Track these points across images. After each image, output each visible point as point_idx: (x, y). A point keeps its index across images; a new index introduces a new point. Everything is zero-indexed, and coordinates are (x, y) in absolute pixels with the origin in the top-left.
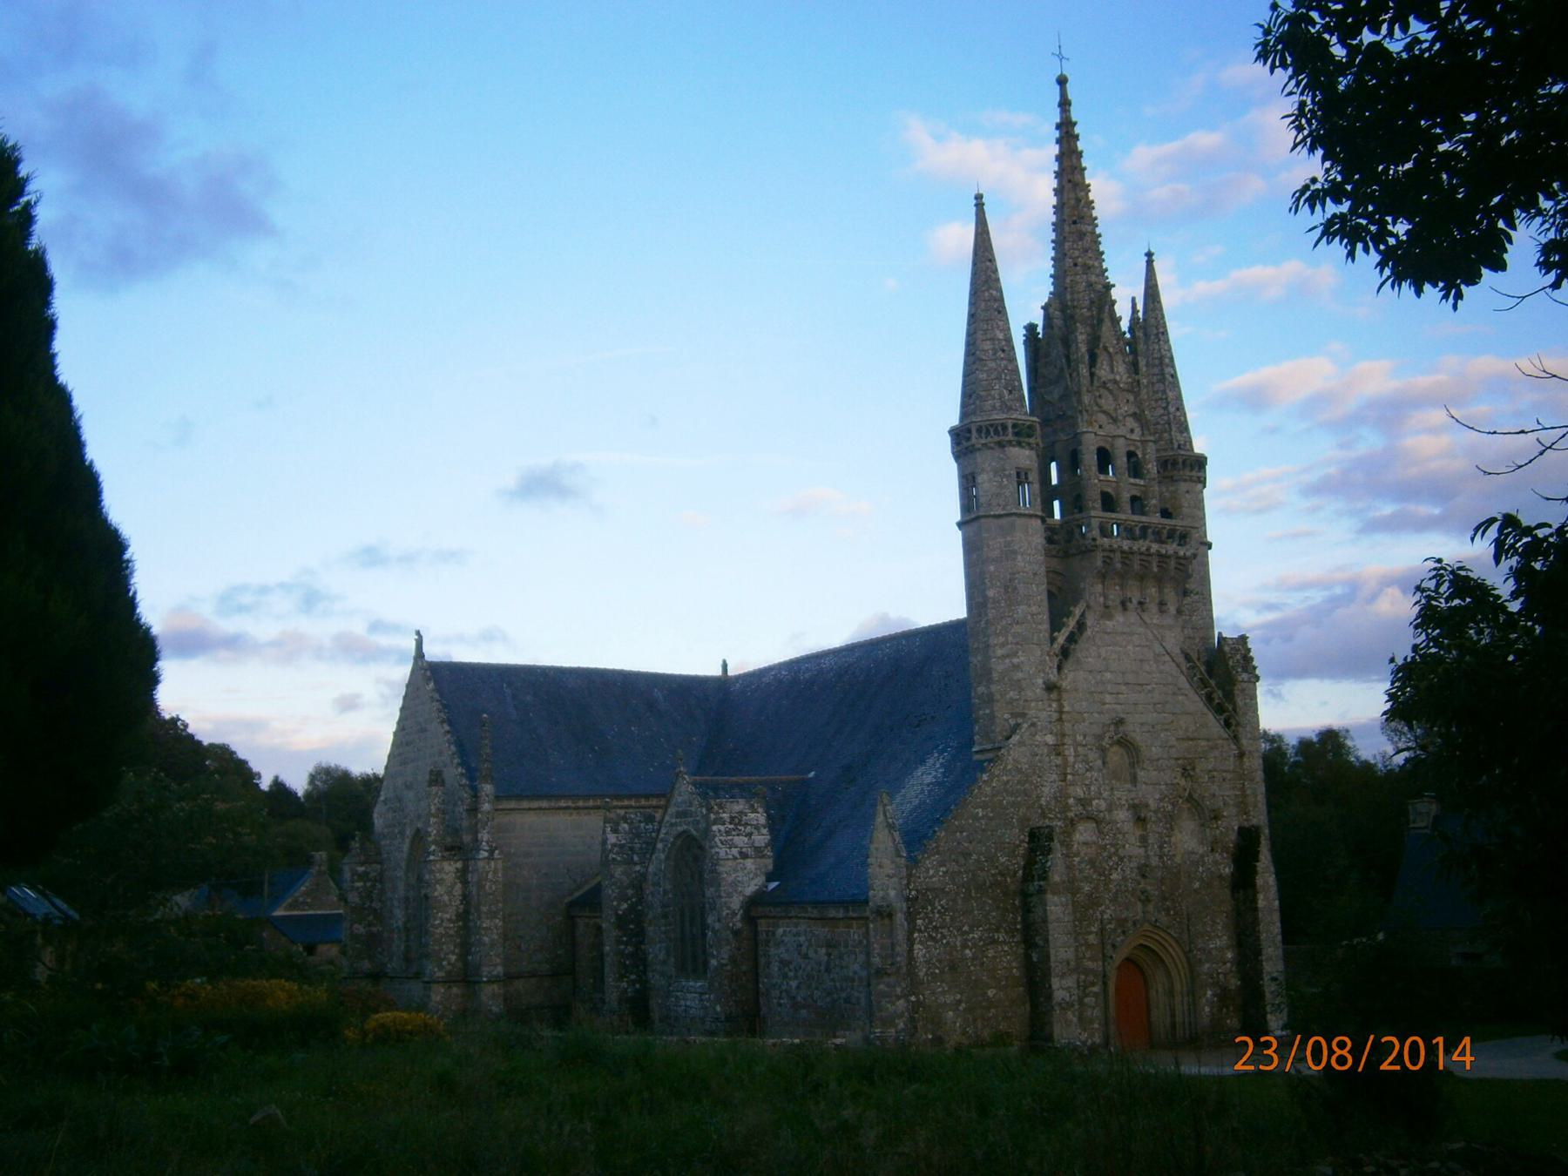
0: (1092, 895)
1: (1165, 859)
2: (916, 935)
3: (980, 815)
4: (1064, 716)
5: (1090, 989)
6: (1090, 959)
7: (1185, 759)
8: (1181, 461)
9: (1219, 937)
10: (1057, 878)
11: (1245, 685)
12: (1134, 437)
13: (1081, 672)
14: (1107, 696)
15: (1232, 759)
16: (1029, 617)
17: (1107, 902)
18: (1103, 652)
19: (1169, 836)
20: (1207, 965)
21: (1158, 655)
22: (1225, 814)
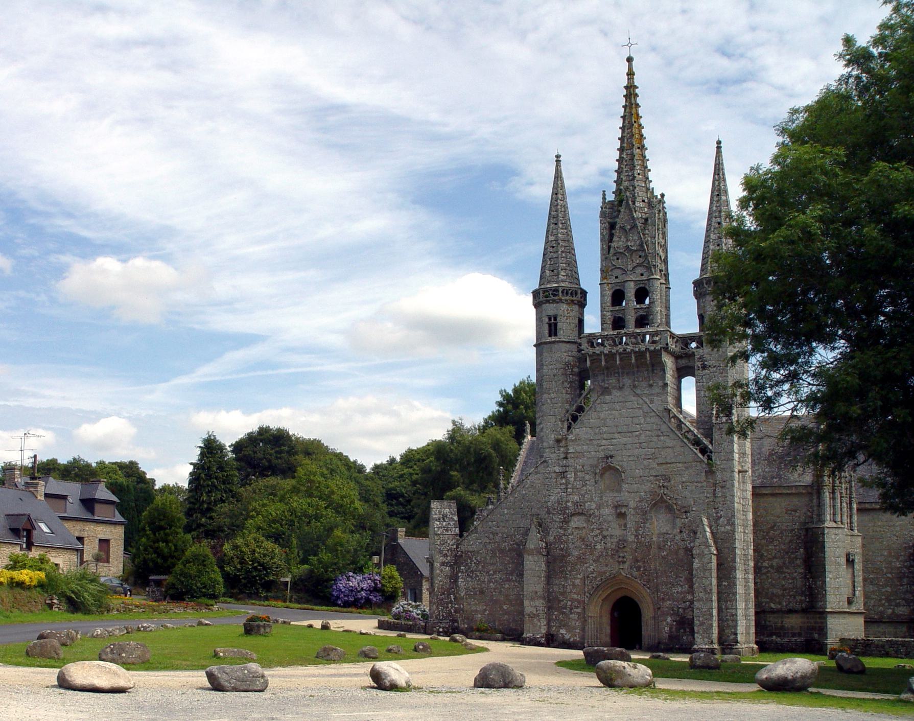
0: (580, 558)
1: (640, 537)
2: (460, 574)
3: (505, 512)
4: (569, 456)
5: (575, 610)
6: (575, 593)
7: (662, 476)
8: (704, 282)
9: (681, 586)
10: (532, 547)
11: (721, 426)
12: (644, 278)
13: (584, 429)
14: (604, 441)
15: (704, 474)
16: (549, 401)
17: (591, 561)
18: (602, 415)
19: (644, 523)
20: (668, 602)
21: (647, 413)
22: (694, 509)
